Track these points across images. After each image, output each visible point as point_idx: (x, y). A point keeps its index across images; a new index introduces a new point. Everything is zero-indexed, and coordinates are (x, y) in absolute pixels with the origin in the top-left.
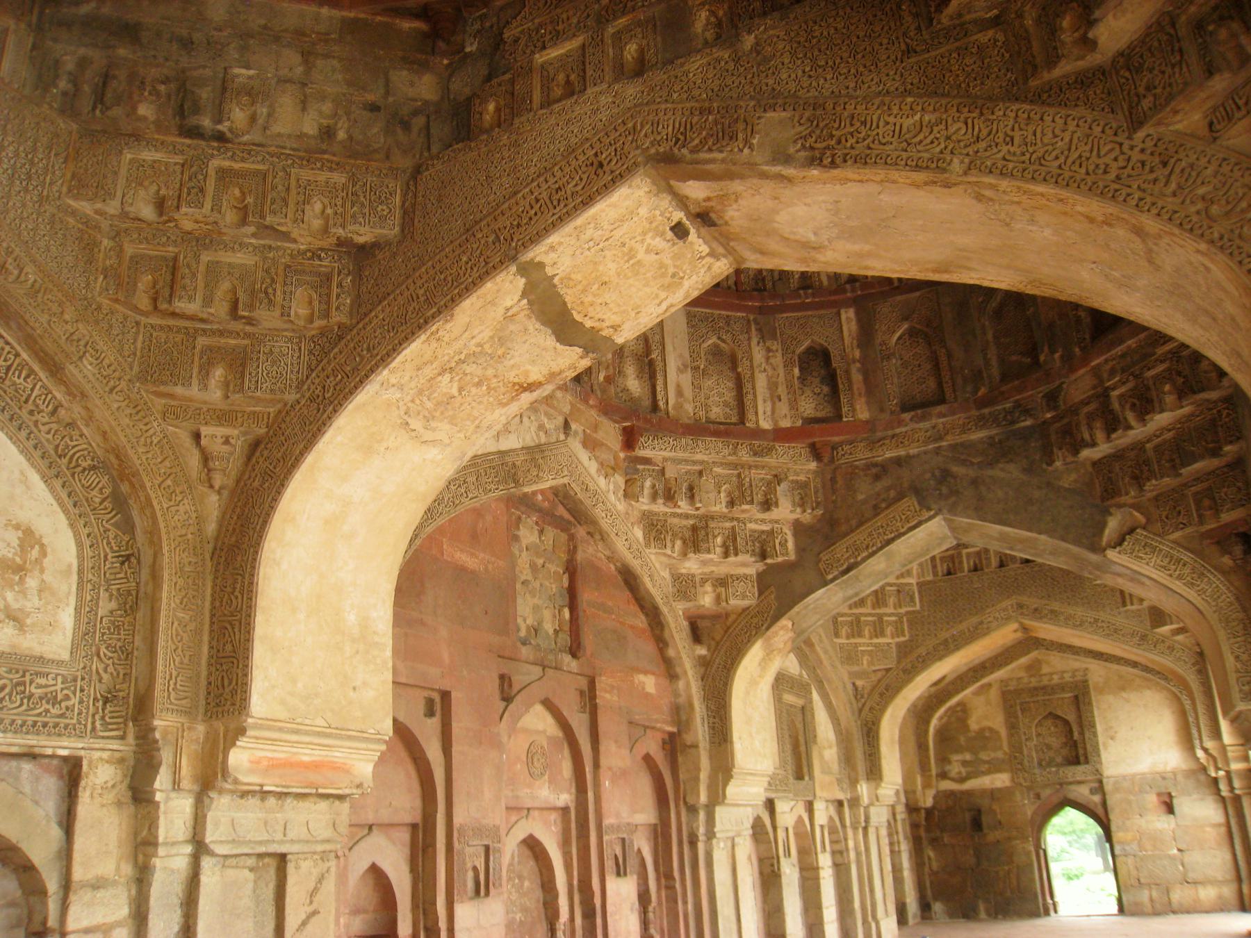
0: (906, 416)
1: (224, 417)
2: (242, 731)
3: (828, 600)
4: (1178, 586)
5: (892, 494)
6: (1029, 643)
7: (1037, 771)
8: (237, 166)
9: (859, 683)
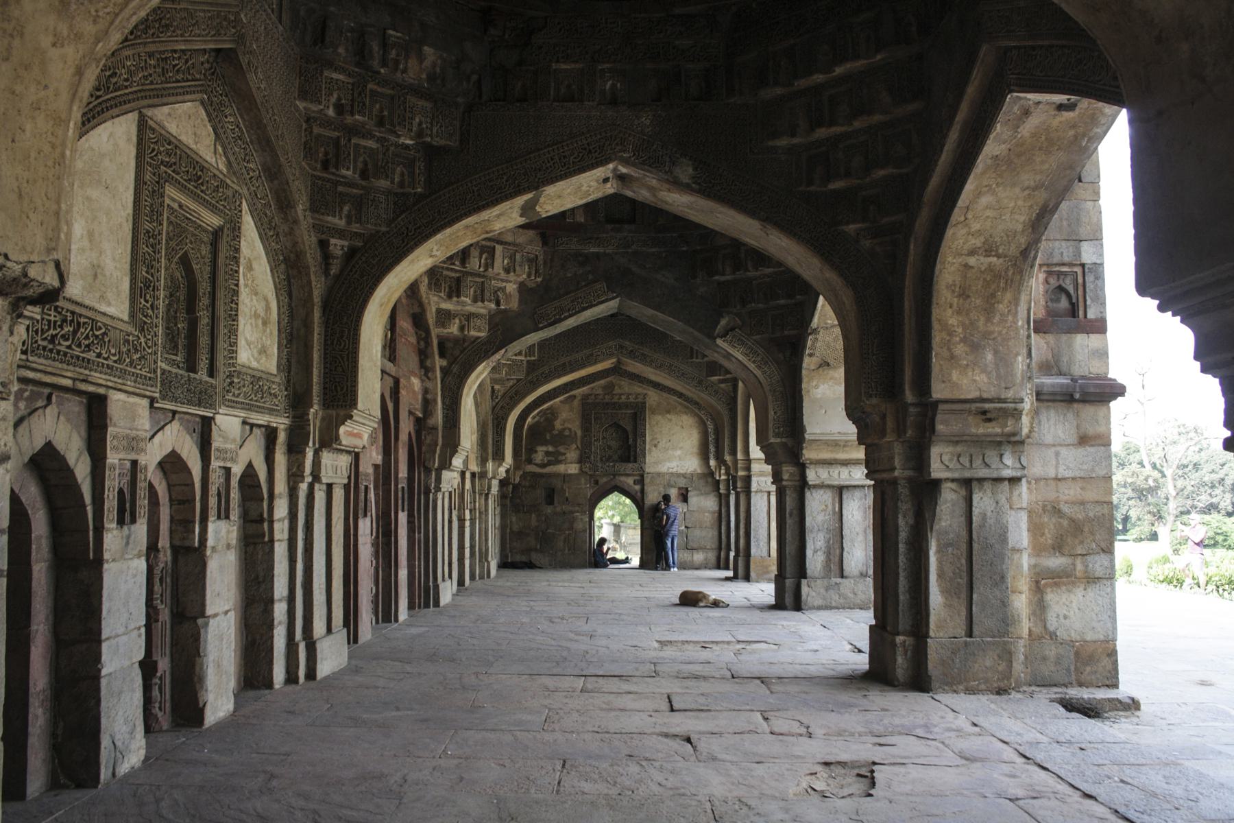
0: (609, 227)
1: (341, 234)
2: (351, 417)
3: (533, 338)
4: (752, 366)
5: (590, 277)
6: (616, 370)
7: (600, 465)
8: (379, 90)
9: (497, 387)
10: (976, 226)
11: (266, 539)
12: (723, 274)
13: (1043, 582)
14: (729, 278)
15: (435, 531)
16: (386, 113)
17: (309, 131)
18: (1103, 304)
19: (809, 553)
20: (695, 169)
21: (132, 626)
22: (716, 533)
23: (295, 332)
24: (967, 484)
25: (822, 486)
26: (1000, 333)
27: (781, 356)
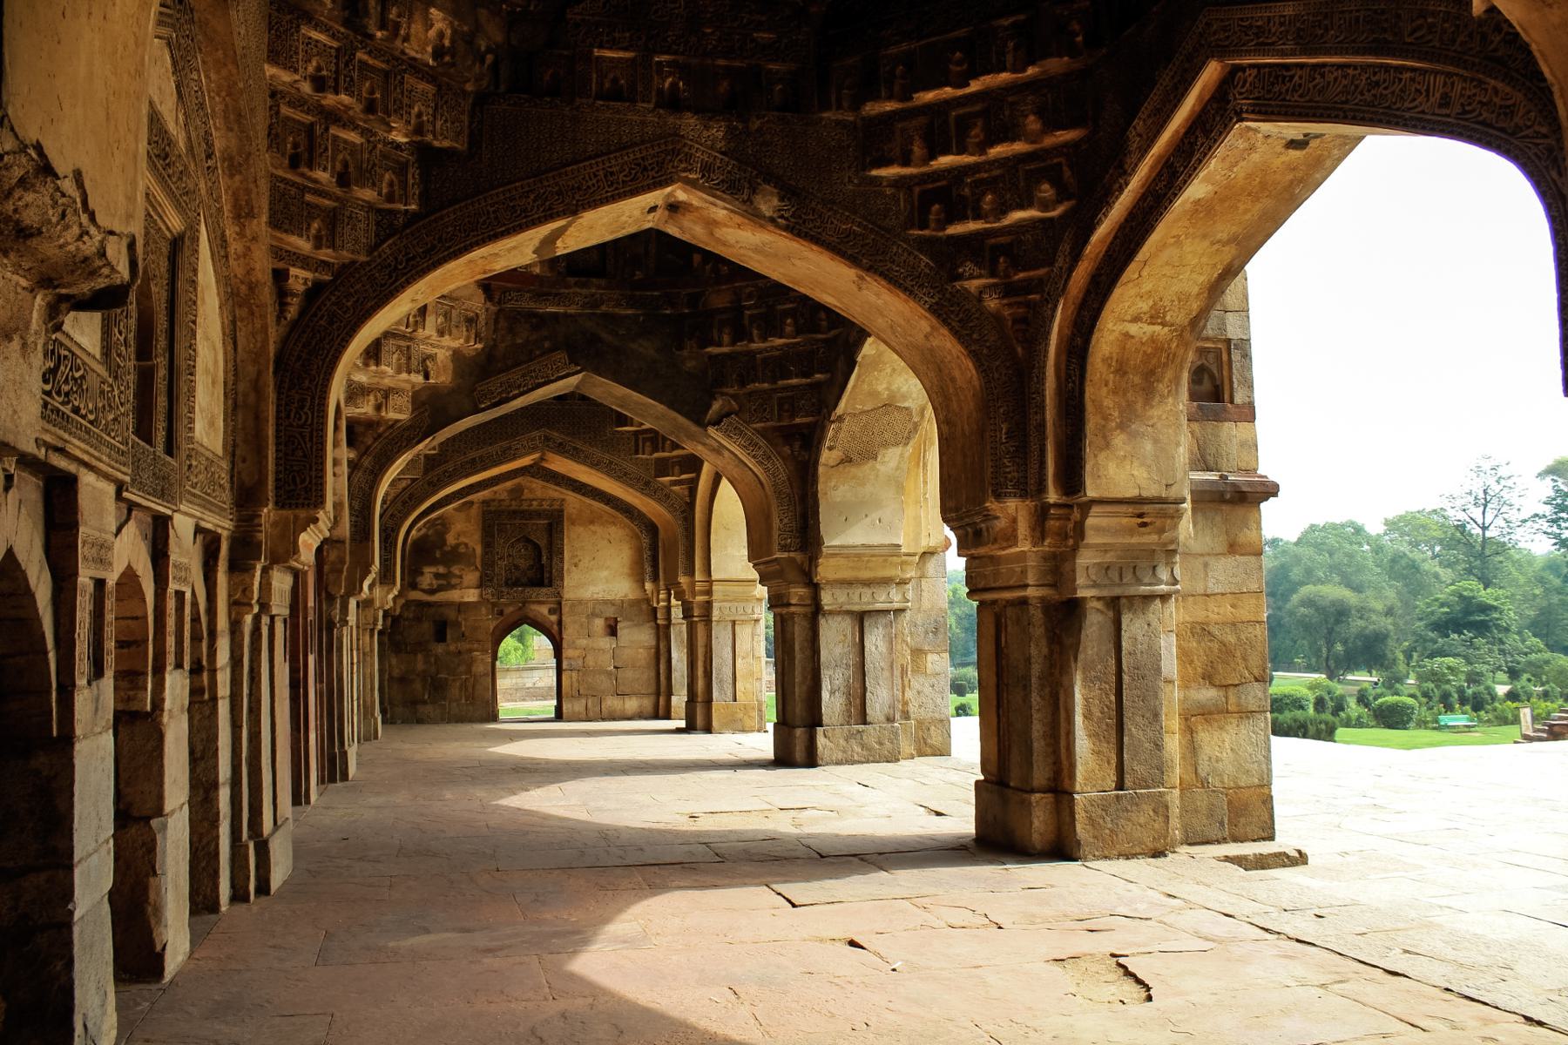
0: (571, 280)
1: (304, 262)
4: (751, 463)
5: (547, 344)
8: (371, 62)
10: (1147, 286)
11: (206, 696)
12: (720, 345)
13: (1195, 716)
14: (725, 350)
15: (340, 679)
16: (378, 95)
17: (274, 110)
18: (1251, 387)
19: (825, 695)
20: (781, 199)
21: (101, 840)
22: (653, 674)
23: (240, 398)
24: (1115, 605)
25: (839, 613)
26: (1160, 418)
27: (787, 450)
